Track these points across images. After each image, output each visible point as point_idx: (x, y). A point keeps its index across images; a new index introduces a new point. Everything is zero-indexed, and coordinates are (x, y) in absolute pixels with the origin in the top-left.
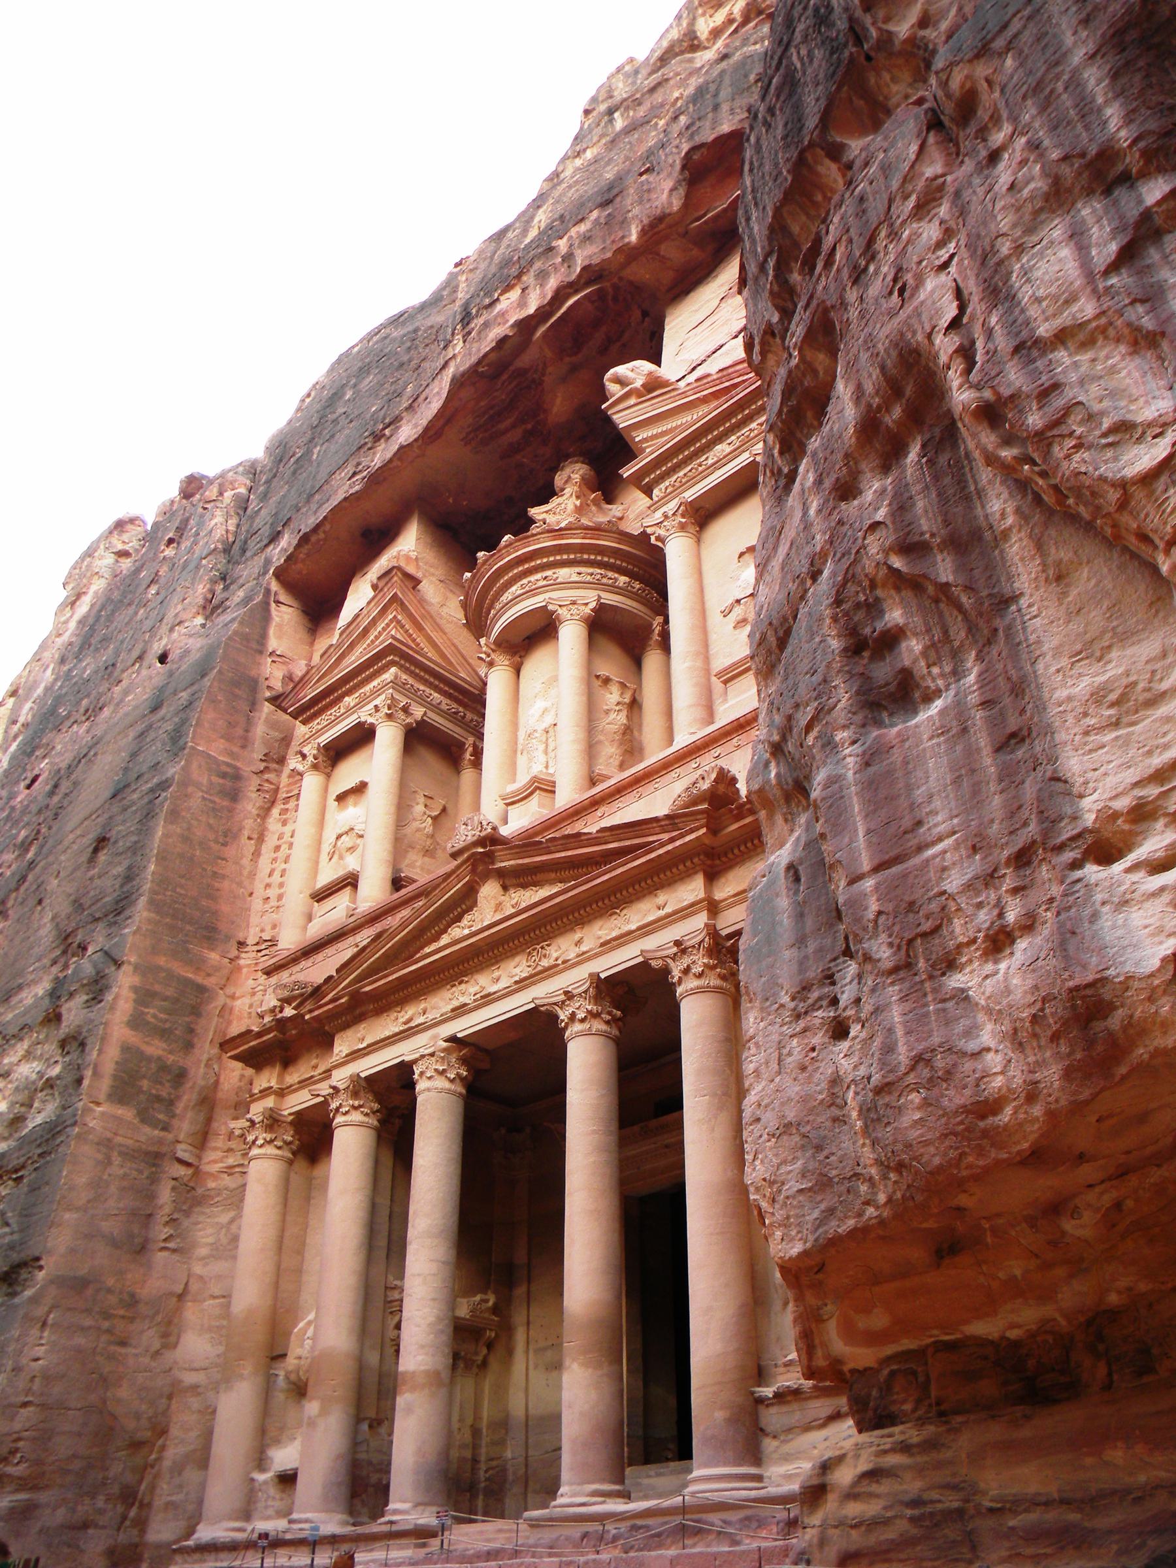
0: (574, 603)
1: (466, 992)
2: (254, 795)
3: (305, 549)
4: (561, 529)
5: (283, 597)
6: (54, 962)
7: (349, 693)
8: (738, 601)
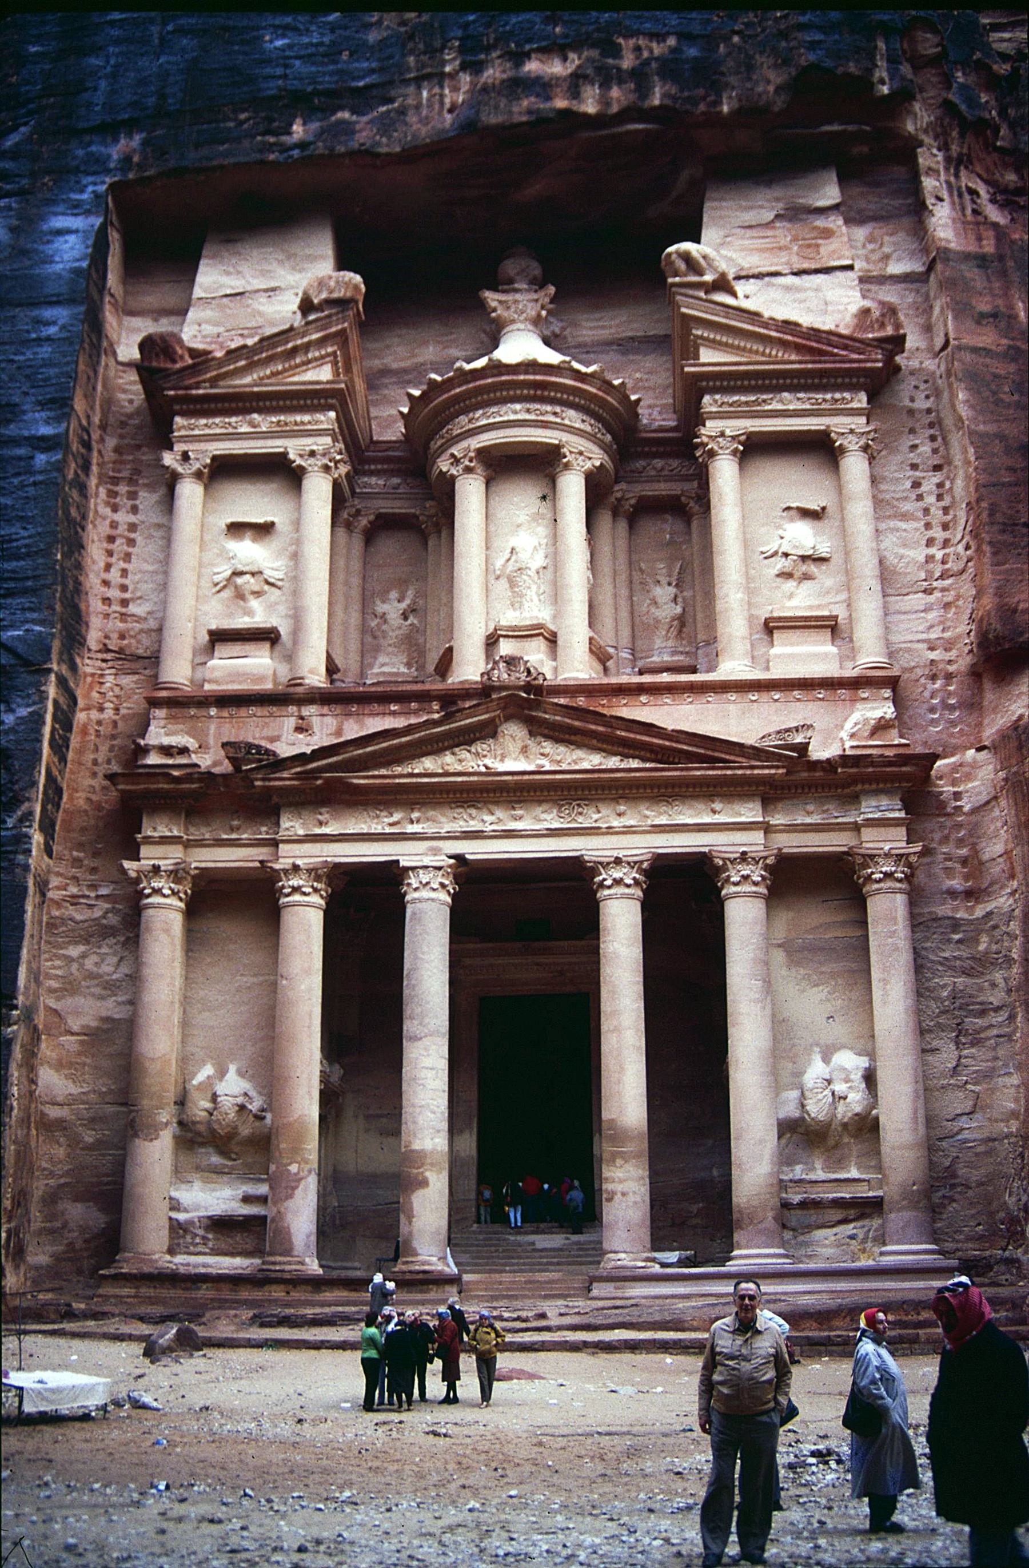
0: (581, 453)
1: (487, 820)
4: (586, 374)
7: (259, 411)
8: (786, 555)
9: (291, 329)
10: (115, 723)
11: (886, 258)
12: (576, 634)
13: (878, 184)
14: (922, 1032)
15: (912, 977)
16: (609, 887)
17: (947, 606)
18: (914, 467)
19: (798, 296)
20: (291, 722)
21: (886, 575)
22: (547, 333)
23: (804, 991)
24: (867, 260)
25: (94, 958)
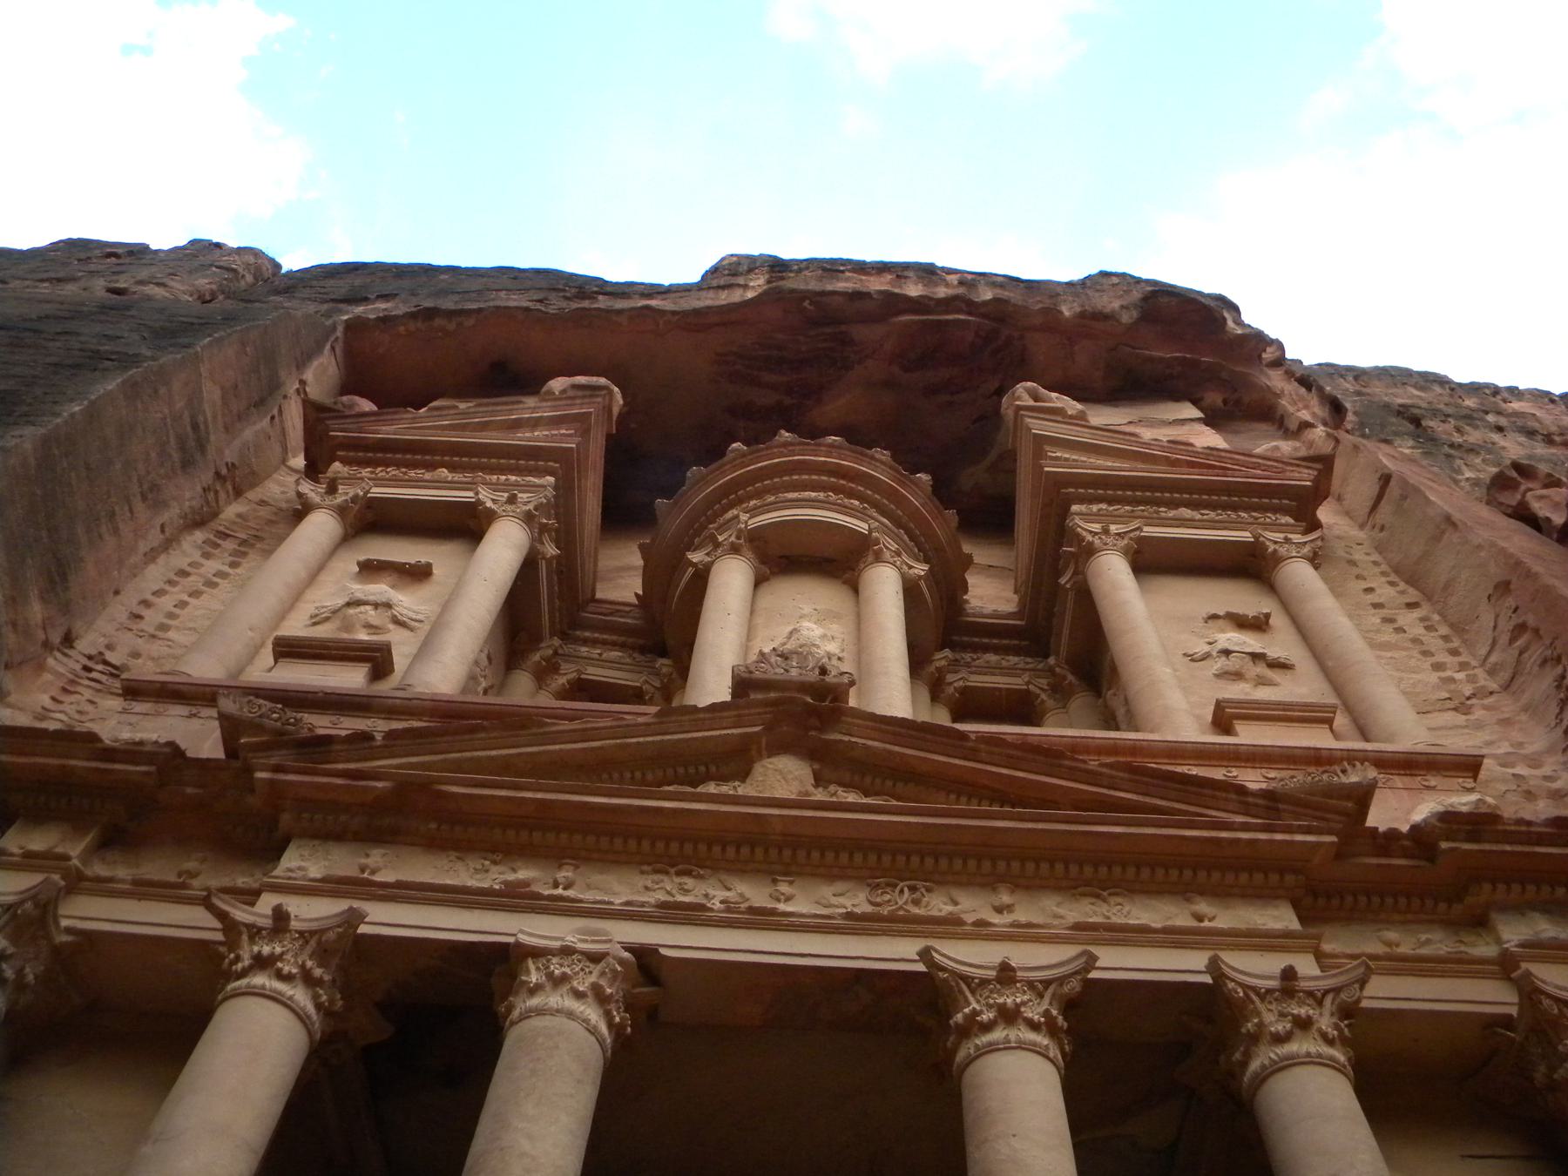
2: (199, 488)
3: (412, 326)
7: (453, 468)
8: (1226, 653)
18: (1376, 606)
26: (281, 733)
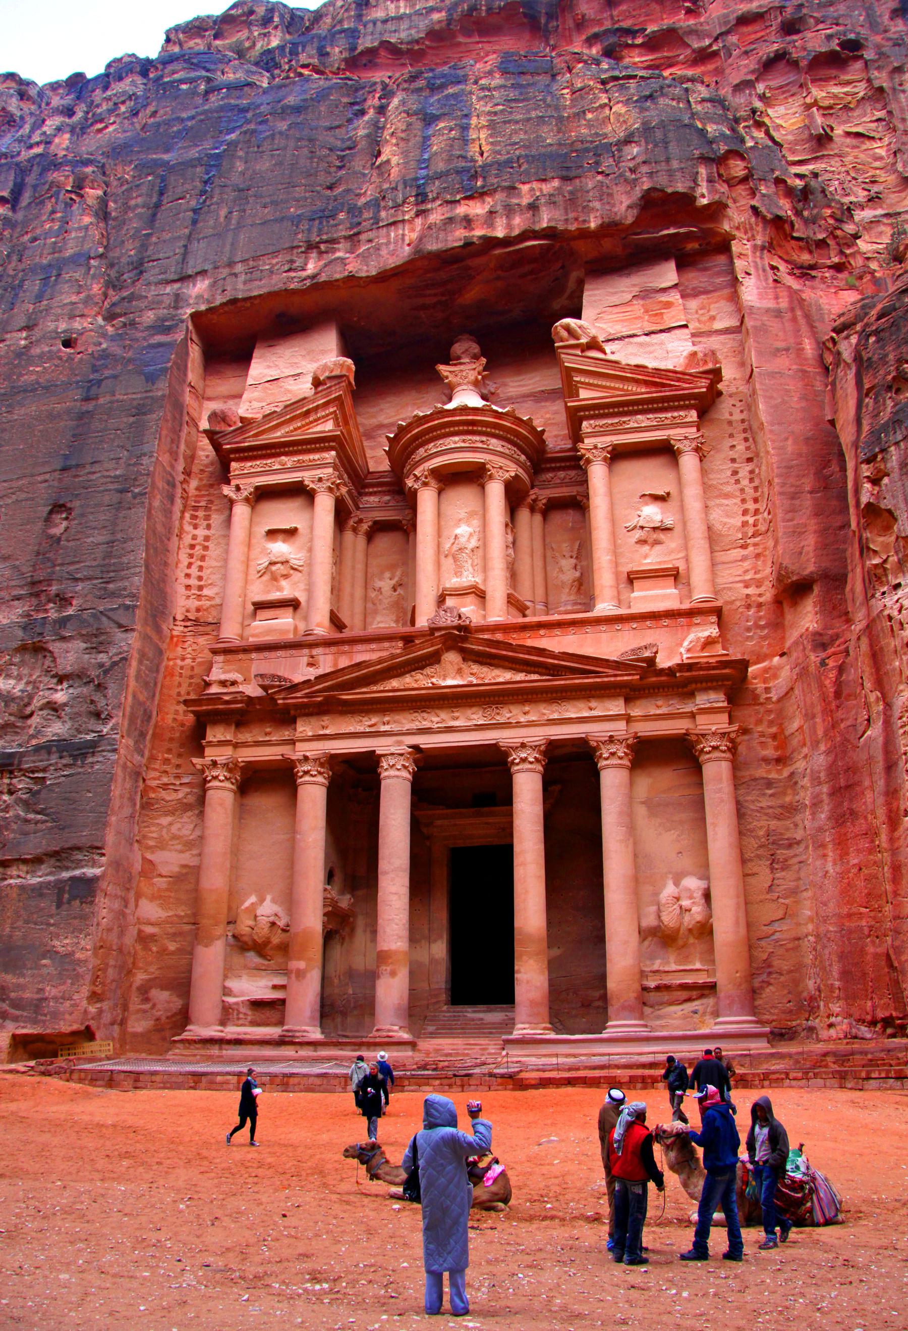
0: (501, 468)
1: (433, 720)
3: (226, 309)
5: (195, 337)
6: (18, 598)
7: (286, 454)
8: (642, 528)
9: (305, 398)
10: (192, 668)
11: (713, 318)
12: (497, 590)
13: (705, 269)
14: (743, 861)
15: (734, 821)
16: (518, 764)
17: (757, 556)
18: (733, 460)
19: (648, 349)
20: (305, 660)
21: (712, 537)
22: (485, 392)
23: (660, 834)
24: (699, 321)
25: (179, 825)
26: (280, 686)
